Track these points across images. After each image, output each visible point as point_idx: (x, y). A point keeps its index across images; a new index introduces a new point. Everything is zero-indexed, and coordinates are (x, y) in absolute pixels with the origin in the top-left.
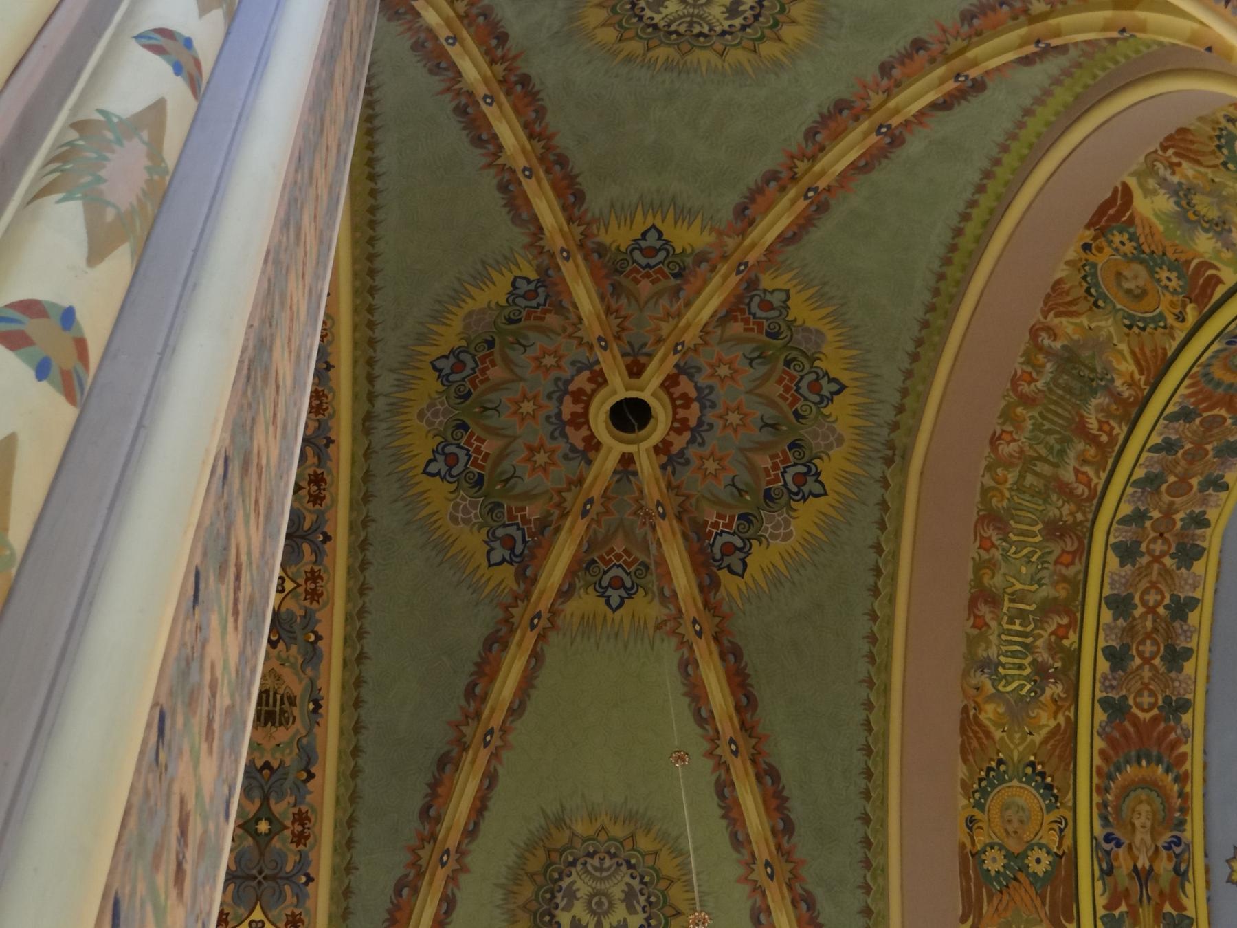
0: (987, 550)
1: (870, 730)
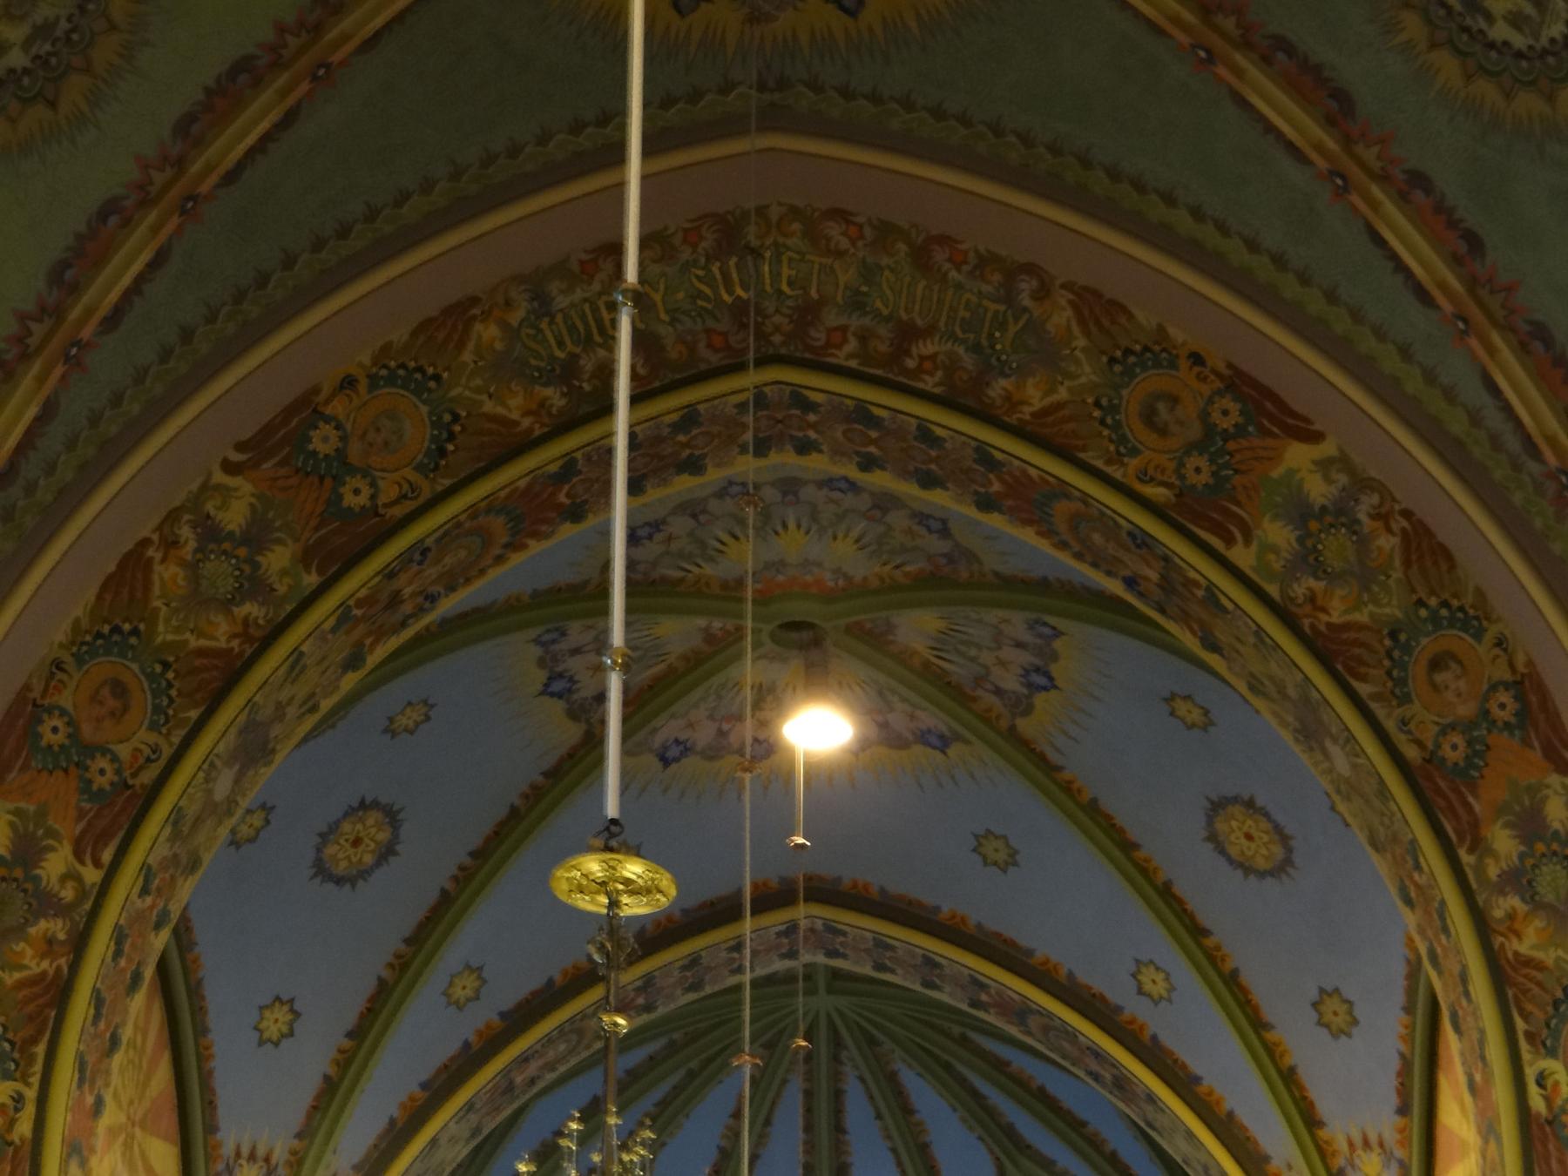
0: (685, 241)
1: (398, 204)
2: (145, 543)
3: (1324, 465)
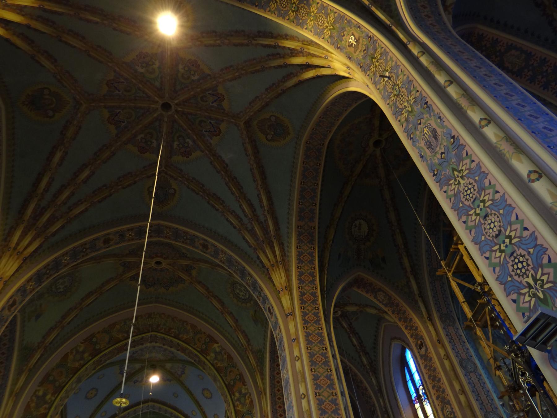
2: (68, 353)
3: (219, 347)
